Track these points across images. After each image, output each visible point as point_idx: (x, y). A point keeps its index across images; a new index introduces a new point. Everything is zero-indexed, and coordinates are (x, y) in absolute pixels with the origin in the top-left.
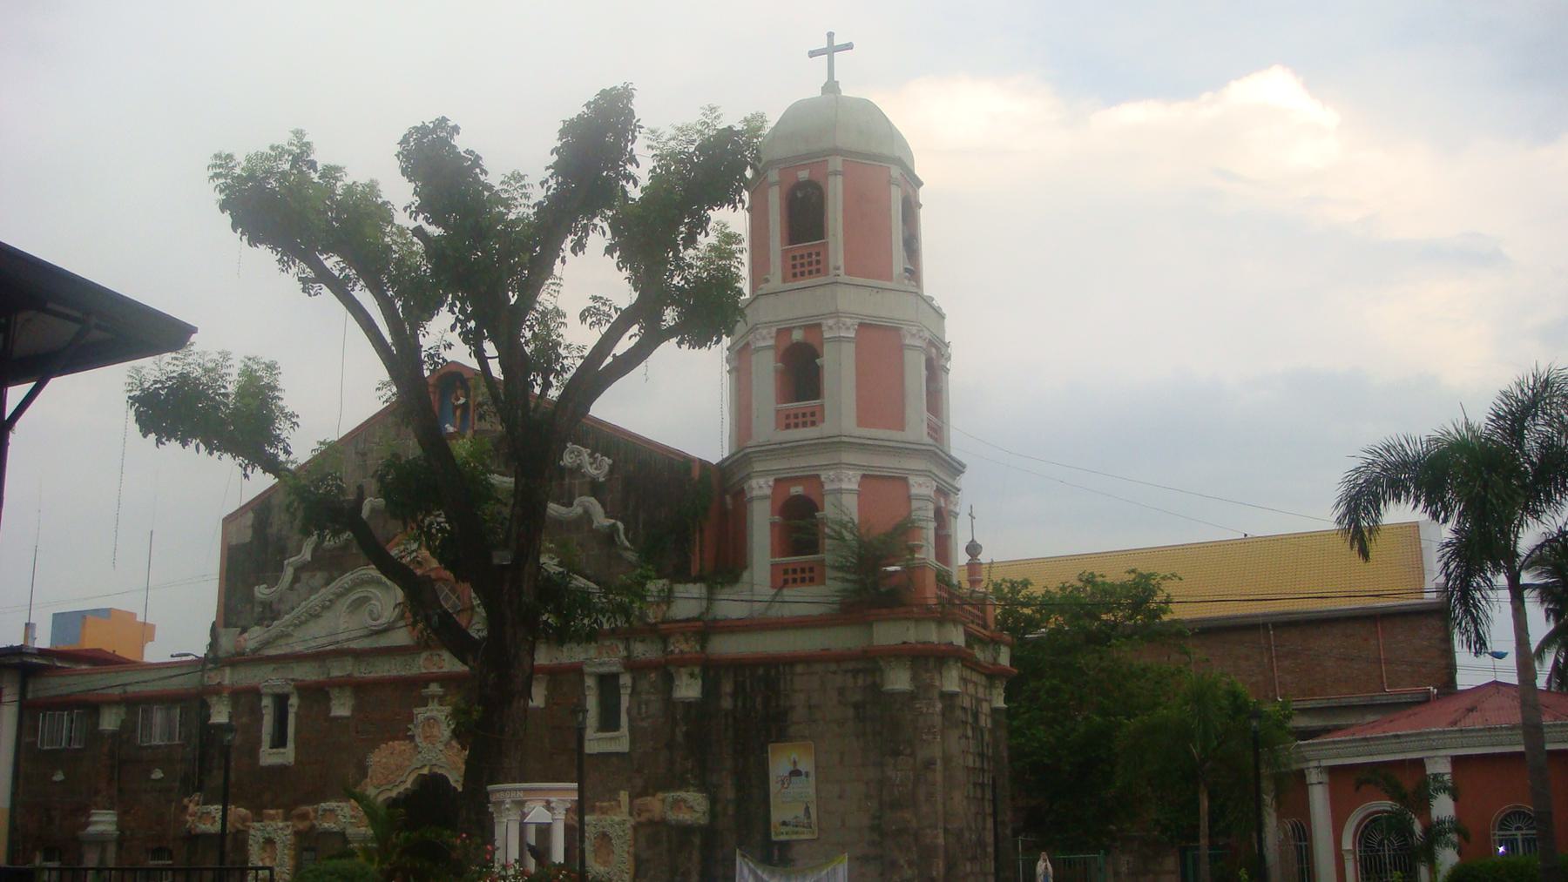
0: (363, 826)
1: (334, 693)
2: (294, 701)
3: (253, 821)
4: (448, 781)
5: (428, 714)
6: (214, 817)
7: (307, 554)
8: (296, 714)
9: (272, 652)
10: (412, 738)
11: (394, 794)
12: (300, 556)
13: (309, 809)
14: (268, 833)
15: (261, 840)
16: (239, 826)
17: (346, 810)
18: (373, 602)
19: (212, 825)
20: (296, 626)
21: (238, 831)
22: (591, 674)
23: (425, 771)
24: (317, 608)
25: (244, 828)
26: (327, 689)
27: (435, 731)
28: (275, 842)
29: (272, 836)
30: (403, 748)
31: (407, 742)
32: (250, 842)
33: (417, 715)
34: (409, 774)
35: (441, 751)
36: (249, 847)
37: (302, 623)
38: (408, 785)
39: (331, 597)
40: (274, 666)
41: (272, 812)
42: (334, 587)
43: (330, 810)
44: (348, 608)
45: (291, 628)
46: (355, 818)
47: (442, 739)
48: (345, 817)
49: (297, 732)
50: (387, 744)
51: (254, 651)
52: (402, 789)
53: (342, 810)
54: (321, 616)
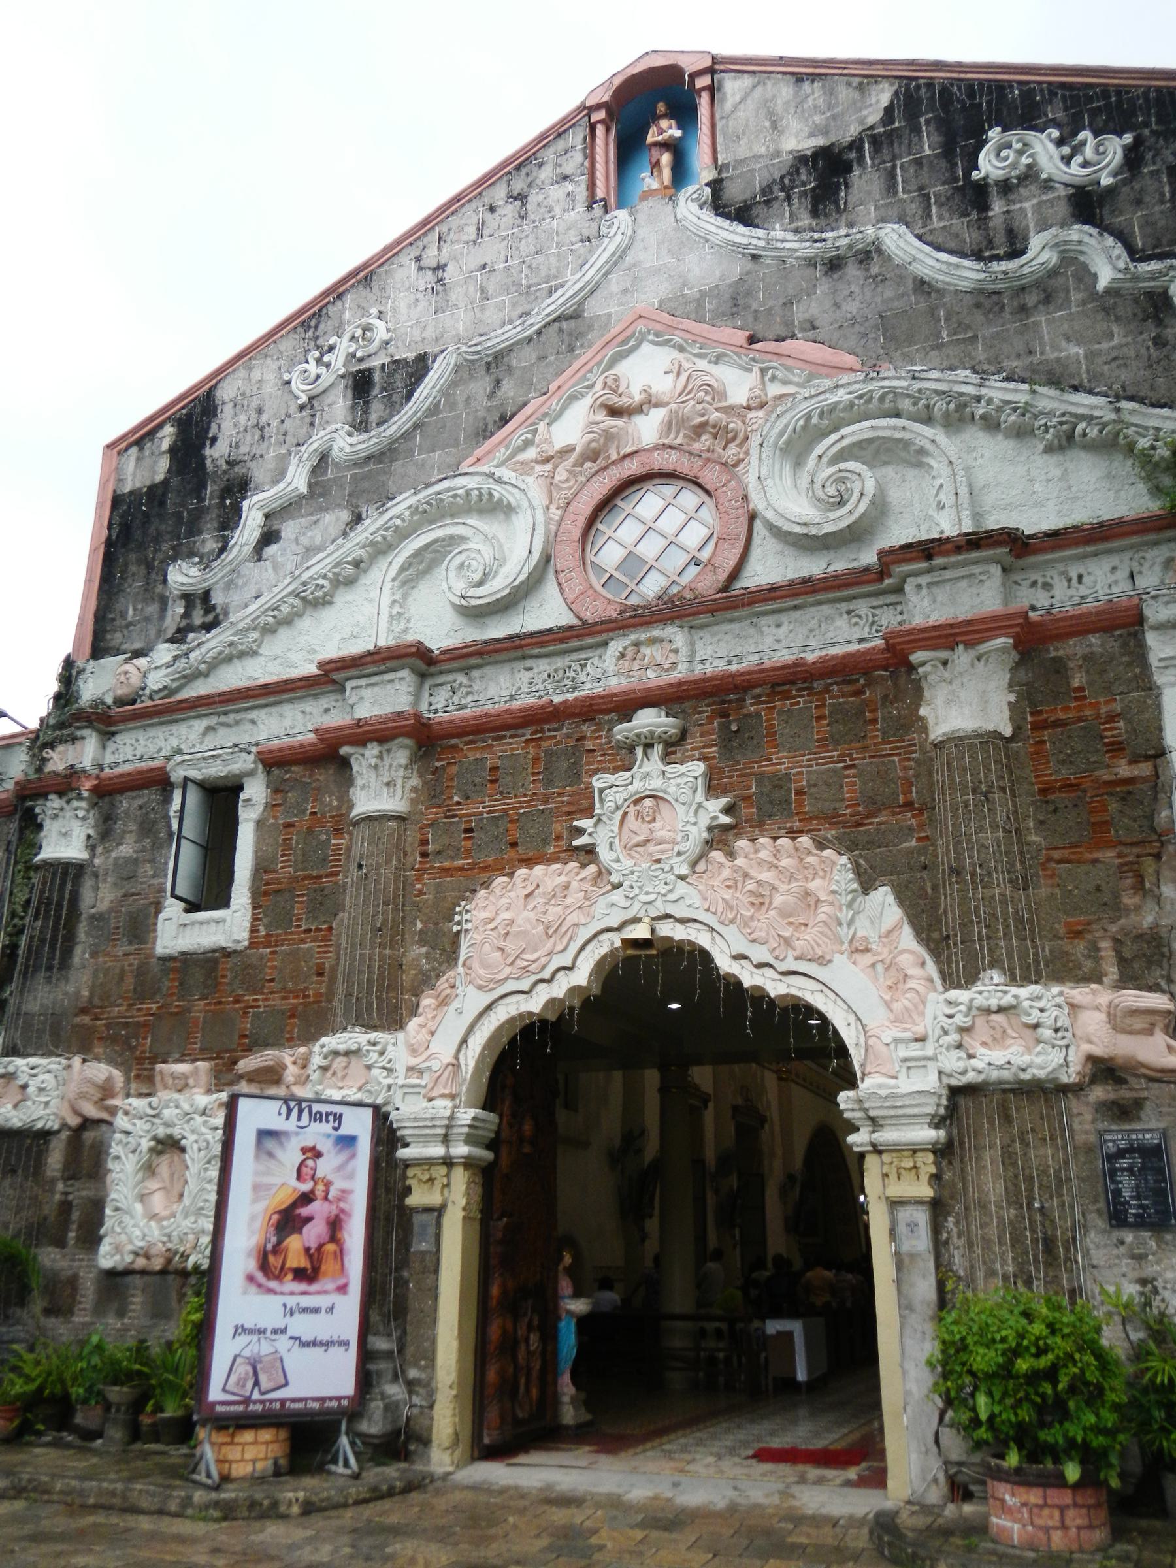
0: (443, 1096)
1: (364, 760)
2: (255, 792)
3: (128, 1096)
4: (705, 956)
5: (638, 785)
6: (24, 1087)
7: (298, 479)
8: (259, 823)
9: (200, 689)
10: (590, 852)
11: (535, 1005)
12: (281, 486)
13: (286, 1057)
14: (167, 1125)
15: (146, 1144)
16: (91, 1111)
17: (391, 1052)
18: (471, 545)
19: (15, 1106)
20: (269, 630)
21: (88, 1123)
22: (1159, 627)
23: (640, 932)
24: (321, 582)
25: (104, 1115)
26: (344, 750)
27: (661, 830)
28: (183, 1150)
29: (176, 1132)
30: (563, 879)
31: (573, 865)
32: (115, 1150)
33: (601, 791)
34: (582, 948)
35: (682, 878)
36: (111, 1165)
37: (288, 621)
38: (581, 977)
39: (359, 553)
40: (205, 723)
41: (182, 1068)
42: (372, 526)
43: (347, 1053)
44: (403, 569)
45: (255, 635)
46: (421, 1072)
47: (682, 847)
48: (390, 1071)
49: (261, 868)
50: (511, 875)
51: (167, 691)
52: (559, 989)
53: (382, 1053)
54: (330, 603)
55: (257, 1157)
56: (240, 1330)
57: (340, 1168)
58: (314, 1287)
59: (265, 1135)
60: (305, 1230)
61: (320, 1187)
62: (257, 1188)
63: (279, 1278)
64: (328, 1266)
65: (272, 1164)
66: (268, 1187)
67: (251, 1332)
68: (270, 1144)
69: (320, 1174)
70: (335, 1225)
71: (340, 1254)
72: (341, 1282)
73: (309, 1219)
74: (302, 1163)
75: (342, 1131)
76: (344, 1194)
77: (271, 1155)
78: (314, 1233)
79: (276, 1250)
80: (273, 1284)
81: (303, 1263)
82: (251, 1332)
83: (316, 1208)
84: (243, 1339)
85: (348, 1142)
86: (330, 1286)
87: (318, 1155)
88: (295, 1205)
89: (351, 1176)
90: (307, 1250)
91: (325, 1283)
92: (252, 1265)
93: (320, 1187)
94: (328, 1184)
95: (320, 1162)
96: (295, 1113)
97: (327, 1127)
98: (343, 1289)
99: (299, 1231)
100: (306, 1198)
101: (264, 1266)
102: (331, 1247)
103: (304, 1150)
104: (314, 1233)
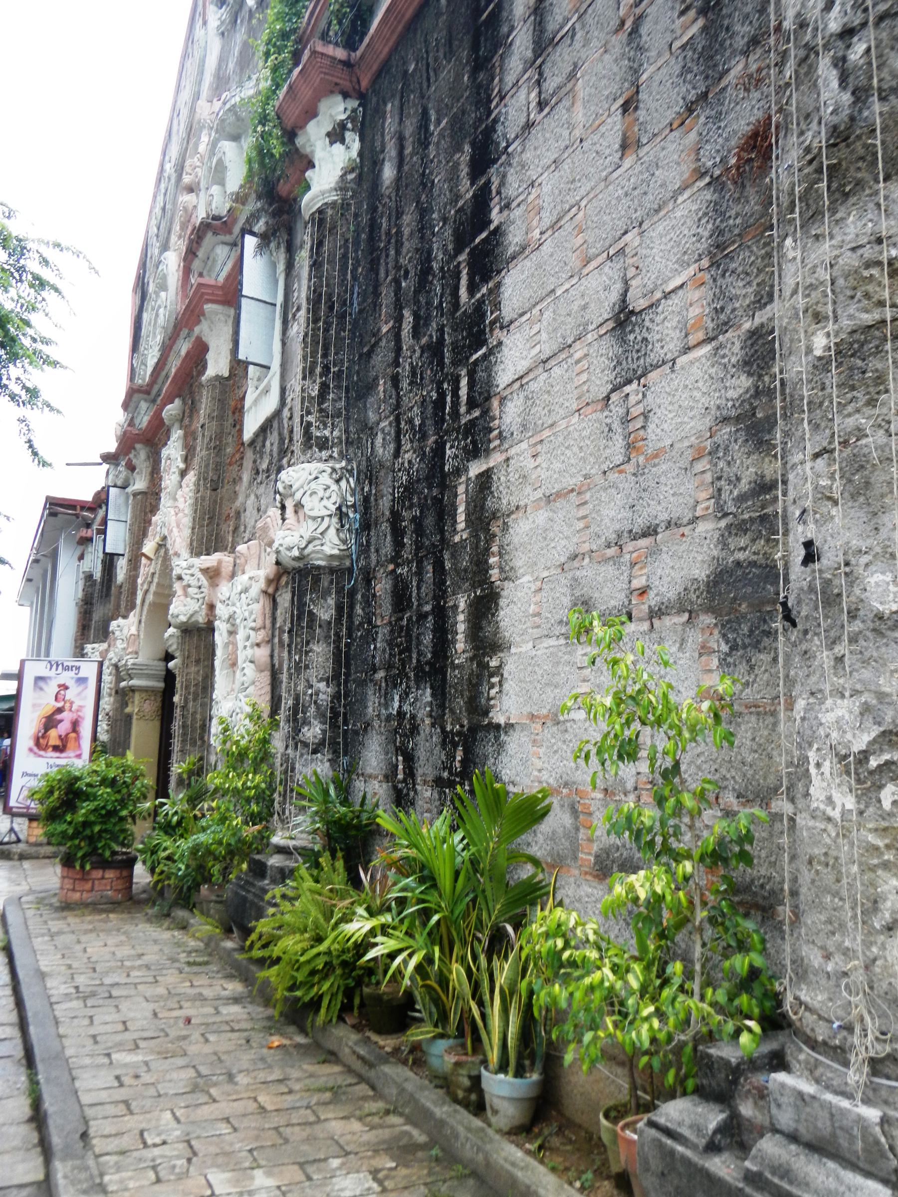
55: (35, 690)
56: (25, 774)
57: (79, 694)
58: (63, 755)
59: (39, 679)
60: (60, 726)
61: (68, 705)
62: (34, 705)
63: (45, 748)
64: (71, 744)
65: (42, 693)
66: (39, 705)
67: (31, 775)
68: (41, 684)
69: (67, 698)
70: (75, 725)
71: (78, 738)
72: (78, 753)
73: (61, 721)
74: (58, 693)
75: (80, 675)
76: (80, 708)
77: (41, 689)
78: (64, 728)
79: (43, 736)
80: (42, 753)
81: (58, 743)
82: (31, 775)
83: (66, 716)
84: (27, 778)
85: (82, 681)
86: (72, 754)
87: (66, 688)
88: (53, 714)
89: (85, 698)
90: (60, 736)
91: (70, 753)
92: (31, 743)
93: (68, 705)
94: (72, 703)
95: (68, 691)
96: (54, 667)
97: (72, 674)
98: (79, 756)
99: (56, 727)
100: (60, 710)
101: (37, 744)
102: (73, 735)
103: (60, 686)
104: (64, 728)
